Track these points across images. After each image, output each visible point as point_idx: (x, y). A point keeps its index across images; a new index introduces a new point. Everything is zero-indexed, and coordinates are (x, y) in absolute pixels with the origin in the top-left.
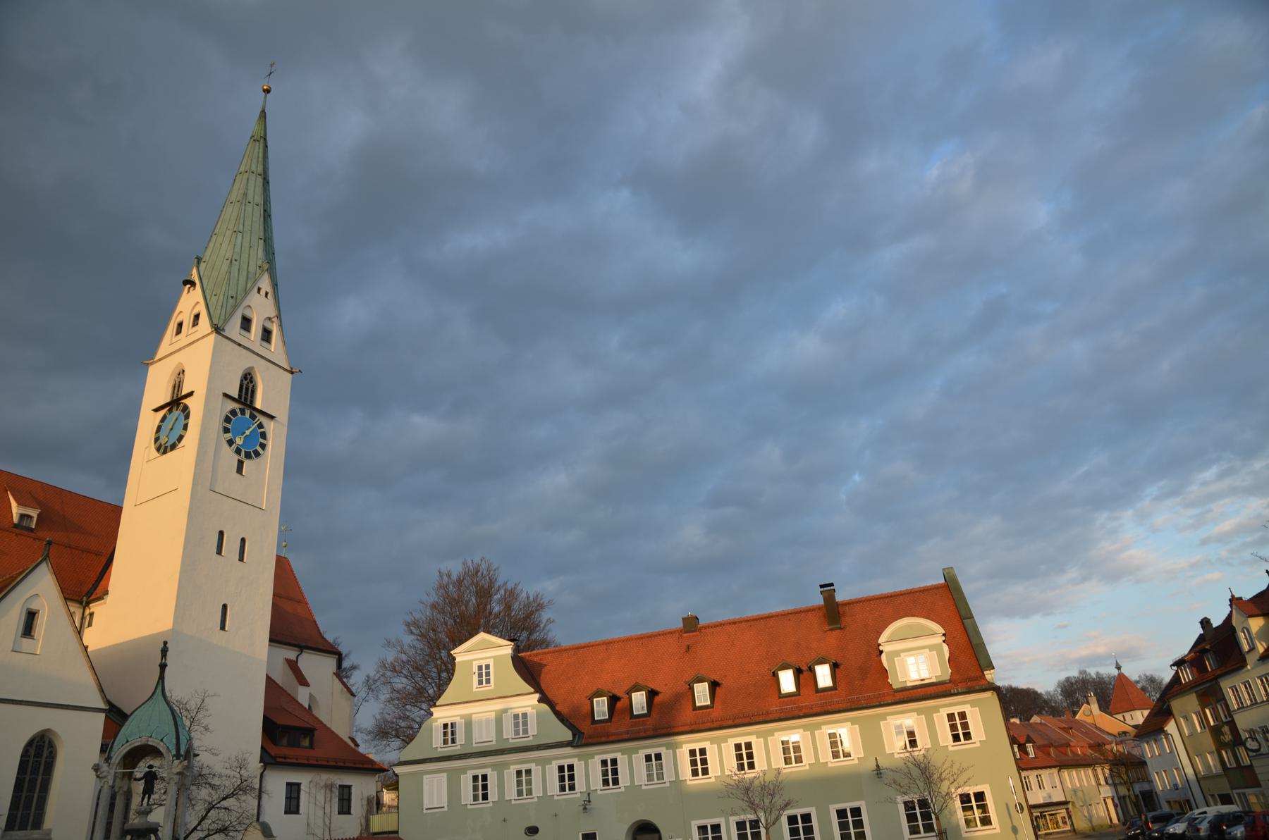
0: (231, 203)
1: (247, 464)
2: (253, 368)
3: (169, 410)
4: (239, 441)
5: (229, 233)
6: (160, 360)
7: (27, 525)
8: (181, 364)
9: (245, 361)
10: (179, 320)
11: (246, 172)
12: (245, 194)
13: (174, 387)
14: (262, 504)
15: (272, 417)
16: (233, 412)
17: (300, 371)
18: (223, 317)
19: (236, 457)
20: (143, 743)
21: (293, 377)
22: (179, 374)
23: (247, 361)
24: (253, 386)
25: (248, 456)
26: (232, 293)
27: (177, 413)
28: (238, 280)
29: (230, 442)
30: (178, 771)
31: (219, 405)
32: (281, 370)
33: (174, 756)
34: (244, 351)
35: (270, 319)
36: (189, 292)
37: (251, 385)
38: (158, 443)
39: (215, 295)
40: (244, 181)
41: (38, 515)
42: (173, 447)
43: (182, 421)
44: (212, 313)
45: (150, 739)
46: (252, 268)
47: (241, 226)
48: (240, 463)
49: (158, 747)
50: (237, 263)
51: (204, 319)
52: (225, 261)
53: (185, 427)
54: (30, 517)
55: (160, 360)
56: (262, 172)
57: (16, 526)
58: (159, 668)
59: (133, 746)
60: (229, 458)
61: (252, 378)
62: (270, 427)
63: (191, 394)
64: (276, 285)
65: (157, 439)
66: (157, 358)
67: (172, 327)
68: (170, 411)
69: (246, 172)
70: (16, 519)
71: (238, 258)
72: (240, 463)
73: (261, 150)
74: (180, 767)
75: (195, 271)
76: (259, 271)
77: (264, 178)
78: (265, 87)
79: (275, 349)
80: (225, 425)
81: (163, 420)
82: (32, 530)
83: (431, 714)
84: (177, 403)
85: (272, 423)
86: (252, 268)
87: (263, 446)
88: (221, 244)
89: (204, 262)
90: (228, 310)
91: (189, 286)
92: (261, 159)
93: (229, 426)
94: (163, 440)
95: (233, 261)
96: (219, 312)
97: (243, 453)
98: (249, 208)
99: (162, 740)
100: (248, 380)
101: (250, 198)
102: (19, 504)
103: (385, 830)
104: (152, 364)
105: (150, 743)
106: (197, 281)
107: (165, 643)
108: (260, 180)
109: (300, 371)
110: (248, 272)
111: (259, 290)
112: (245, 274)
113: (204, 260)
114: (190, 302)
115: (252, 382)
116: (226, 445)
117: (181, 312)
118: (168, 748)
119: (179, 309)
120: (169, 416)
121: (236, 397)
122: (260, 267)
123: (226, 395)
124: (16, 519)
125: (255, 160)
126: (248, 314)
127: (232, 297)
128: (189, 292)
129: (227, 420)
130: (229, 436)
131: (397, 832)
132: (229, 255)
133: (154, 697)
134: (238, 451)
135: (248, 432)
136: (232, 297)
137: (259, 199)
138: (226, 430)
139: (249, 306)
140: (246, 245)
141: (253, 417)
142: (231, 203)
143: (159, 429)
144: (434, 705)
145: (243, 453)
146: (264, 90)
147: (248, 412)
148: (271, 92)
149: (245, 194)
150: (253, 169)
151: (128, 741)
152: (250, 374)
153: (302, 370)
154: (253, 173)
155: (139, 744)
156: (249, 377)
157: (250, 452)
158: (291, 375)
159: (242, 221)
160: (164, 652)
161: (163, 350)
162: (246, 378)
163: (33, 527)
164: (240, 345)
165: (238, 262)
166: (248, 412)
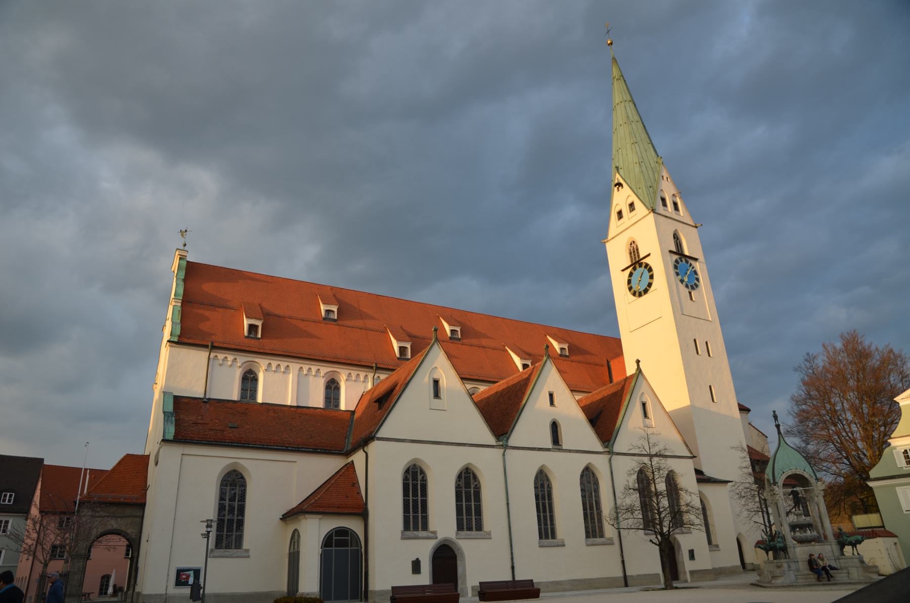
0: (621, 125)
3: (633, 268)
4: (686, 279)
5: (628, 146)
6: (613, 238)
8: (632, 238)
9: (671, 227)
10: (618, 209)
11: (622, 102)
12: (628, 117)
13: (631, 253)
14: (709, 318)
15: (696, 259)
16: (676, 261)
17: (701, 225)
18: (651, 201)
19: (687, 290)
20: (794, 473)
21: (698, 231)
22: (631, 244)
23: (671, 227)
25: (693, 288)
26: (649, 184)
27: (640, 270)
28: (648, 174)
29: (682, 281)
30: (823, 488)
31: (669, 257)
32: (691, 228)
33: (815, 480)
34: (670, 220)
35: (674, 195)
36: (618, 190)
37: (678, 241)
38: (632, 291)
39: (640, 188)
40: (623, 109)
42: (646, 291)
43: (647, 274)
44: (643, 201)
45: (797, 470)
46: (653, 165)
47: (635, 140)
48: (690, 293)
49: (804, 474)
51: (638, 204)
52: (635, 165)
53: (652, 277)
54: (564, 349)
55: (613, 238)
56: (631, 99)
57: (561, 355)
58: (775, 428)
59: (787, 475)
60: (684, 291)
61: (677, 236)
62: (697, 266)
63: (649, 255)
65: (630, 289)
66: (610, 237)
67: (614, 216)
68: (635, 269)
69: (622, 102)
70: (559, 351)
71: (642, 161)
72: (690, 293)
73: (624, 84)
74: (824, 486)
75: (617, 175)
76: (657, 165)
77: (634, 103)
78: (609, 42)
79: (683, 214)
80: (676, 270)
81: (631, 275)
82: (568, 356)
83: (890, 444)
84: (637, 263)
85: (697, 264)
86: (653, 165)
87: (698, 280)
88: (627, 154)
89: (621, 168)
90: (652, 196)
91: (617, 186)
92: (626, 91)
93: (678, 271)
94: (635, 287)
95: (641, 163)
96: (647, 199)
97: (690, 287)
98: (634, 126)
99: (804, 470)
101: (632, 119)
102: (559, 342)
103: (869, 525)
104: (607, 241)
105: (798, 473)
106: (622, 181)
107: (774, 412)
108: (631, 104)
110: (652, 168)
111: (663, 177)
112: (650, 169)
113: (620, 168)
114: (621, 198)
115: (678, 239)
116: (680, 283)
117: (617, 204)
118: (810, 475)
119: (614, 203)
120: (635, 273)
121: (675, 251)
123: (671, 252)
124: (559, 351)
125: (623, 93)
127: (650, 187)
128: (618, 190)
129: (676, 267)
130: (680, 277)
131: (883, 527)
132: (636, 160)
133: (781, 445)
134: (687, 286)
135: (688, 273)
136: (650, 187)
137: (636, 118)
138: (677, 274)
140: (643, 150)
141: (687, 262)
142: (621, 125)
143: (629, 282)
144: (890, 438)
145: (690, 287)
146: (609, 45)
147: (683, 260)
148: (613, 43)
149: (628, 117)
150: (625, 99)
151: (784, 472)
154: (626, 101)
155: (791, 473)
156: (675, 236)
157: (693, 286)
158: (696, 229)
159: (633, 135)
160: (776, 417)
161: (612, 231)
164: (666, 217)
166: (683, 260)
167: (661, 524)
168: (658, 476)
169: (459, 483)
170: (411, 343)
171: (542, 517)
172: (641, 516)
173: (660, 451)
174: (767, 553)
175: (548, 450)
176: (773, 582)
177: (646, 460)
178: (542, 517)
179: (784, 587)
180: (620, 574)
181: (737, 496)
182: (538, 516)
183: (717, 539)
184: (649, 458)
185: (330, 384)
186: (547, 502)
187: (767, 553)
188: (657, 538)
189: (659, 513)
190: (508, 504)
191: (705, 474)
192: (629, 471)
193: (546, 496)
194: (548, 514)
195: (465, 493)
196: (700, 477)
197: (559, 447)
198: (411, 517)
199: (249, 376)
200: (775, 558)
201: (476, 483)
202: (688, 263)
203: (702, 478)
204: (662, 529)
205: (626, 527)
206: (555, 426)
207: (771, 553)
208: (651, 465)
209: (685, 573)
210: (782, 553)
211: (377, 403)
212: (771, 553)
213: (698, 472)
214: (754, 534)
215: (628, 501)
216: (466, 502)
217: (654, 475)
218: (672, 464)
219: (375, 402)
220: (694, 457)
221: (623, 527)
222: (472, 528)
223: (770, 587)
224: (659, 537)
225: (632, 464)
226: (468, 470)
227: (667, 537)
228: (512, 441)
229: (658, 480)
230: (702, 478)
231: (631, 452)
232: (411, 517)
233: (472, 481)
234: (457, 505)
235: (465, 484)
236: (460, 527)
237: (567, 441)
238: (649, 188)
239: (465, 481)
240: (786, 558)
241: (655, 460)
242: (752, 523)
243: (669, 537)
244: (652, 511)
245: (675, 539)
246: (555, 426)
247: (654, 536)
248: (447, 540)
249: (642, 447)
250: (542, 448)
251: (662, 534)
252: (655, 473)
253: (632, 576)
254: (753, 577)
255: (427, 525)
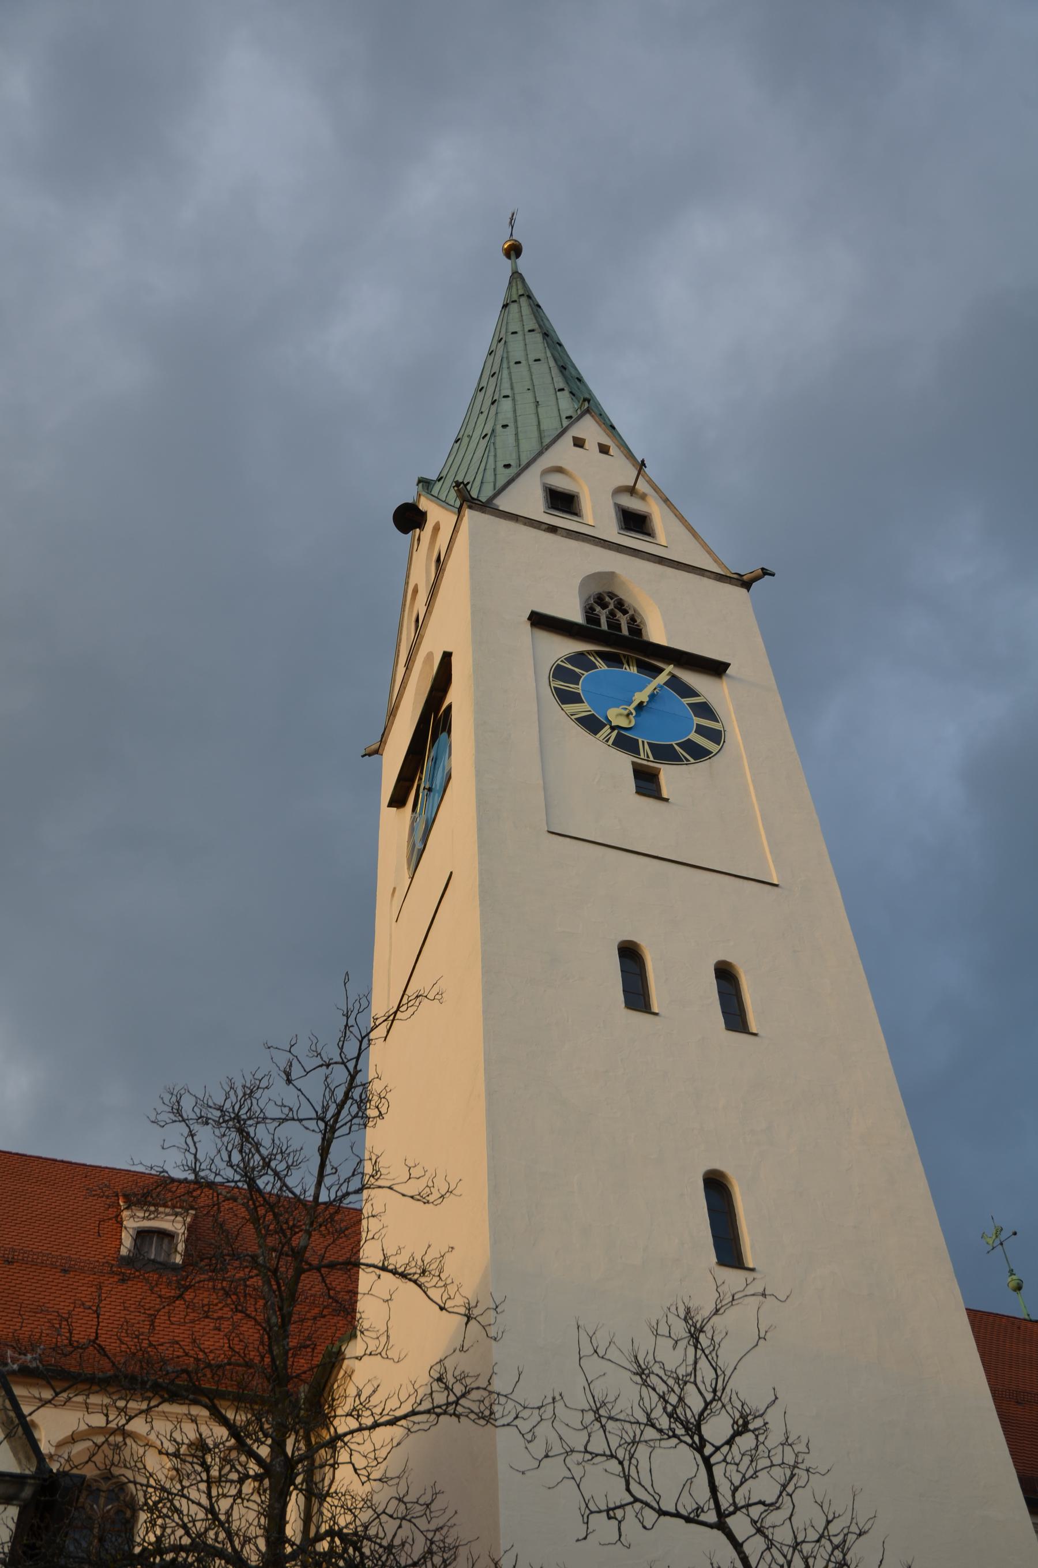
1: (669, 775)
2: (612, 575)
7: (162, 1258)
15: (717, 669)
24: (633, 619)
25: (665, 754)
29: (591, 724)
41: (191, 1229)
50: (511, 430)
57: (128, 1261)
64: (613, 427)
95: (499, 428)
97: (645, 750)
100: (611, 607)
109: (765, 572)
123: (540, 621)
126: (560, 483)
134: (625, 743)
139: (559, 470)
145: (645, 750)
152: (612, 595)
153: (770, 568)
162: (600, 600)
163: (178, 1259)
165: (511, 430)
238: (500, 469)
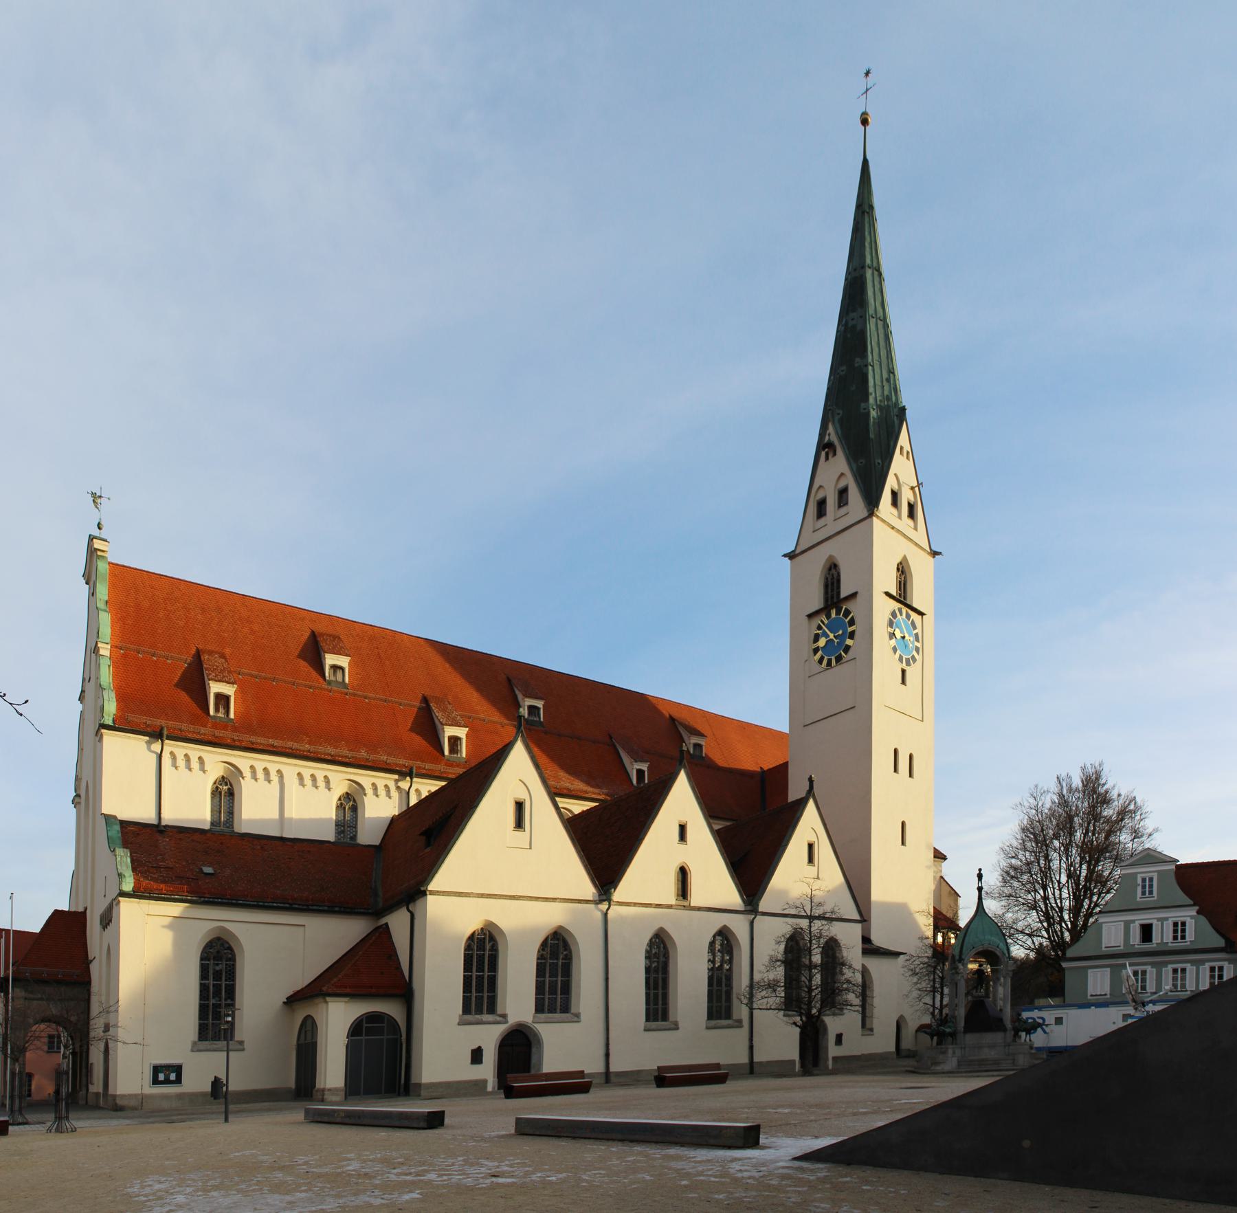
122: (897, 416)
167: (810, 1002)
168: (815, 946)
169: (542, 952)
170: (467, 729)
171: (652, 995)
172: (783, 995)
173: (824, 913)
174: (932, 1039)
175: (670, 907)
176: (933, 1068)
177: (804, 923)
178: (652, 995)
179: (943, 1073)
180: (746, 1060)
181: (910, 973)
182: (646, 993)
183: (876, 1024)
184: (808, 921)
185: (343, 802)
186: (660, 976)
187: (932, 1039)
188: (801, 1020)
189: (810, 990)
190: (607, 979)
191: (873, 943)
192: (778, 937)
193: (660, 969)
194: (660, 991)
195: (550, 965)
196: (867, 946)
197: (686, 903)
198: (474, 999)
199: (221, 787)
200: (939, 1043)
201: (565, 953)
202: (909, 620)
203: (869, 948)
204: (810, 1009)
205: (764, 1007)
206: (683, 873)
207: (935, 1038)
208: (810, 931)
209: (827, 1059)
210: (950, 1039)
211: (424, 838)
212: (935, 1038)
213: (866, 940)
214: (918, 1017)
215: (771, 976)
216: (550, 977)
217: (811, 943)
218: (837, 930)
219: (420, 835)
220: (865, 921)
221: (761, 1007)
222: (555, 1009)
223: (928, 1074)
224: (804, 1018)
225: (783, 928)
226: (557, 935)
227: (814, 1020)
228: (619, 894)
229: (816, 950)
230: (869, 948)
231: (785, 912)
232: (474, 999)
233: (561, 949)
234: (537, 981)
235: (550, 954)
236: (539, 1008)
237: (696, 898)
239: (551, 950)
240: (952, 1044)
241: (817, 924)
242: (921, 1004)
243: (817, 1021)
244: (799, 988)
245: (823, 1021)
246: (683, 873)
247: (798, 1019)
248: (523, 1025)
249: (801, 907)
250: (660, 905)
251: (809, 1016)
252: (814, 942)
253: (760, 1063)
254: (911, 1062)
255: (494, 1006)
